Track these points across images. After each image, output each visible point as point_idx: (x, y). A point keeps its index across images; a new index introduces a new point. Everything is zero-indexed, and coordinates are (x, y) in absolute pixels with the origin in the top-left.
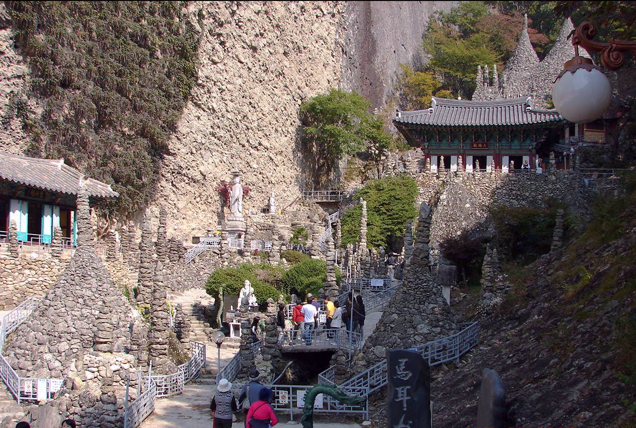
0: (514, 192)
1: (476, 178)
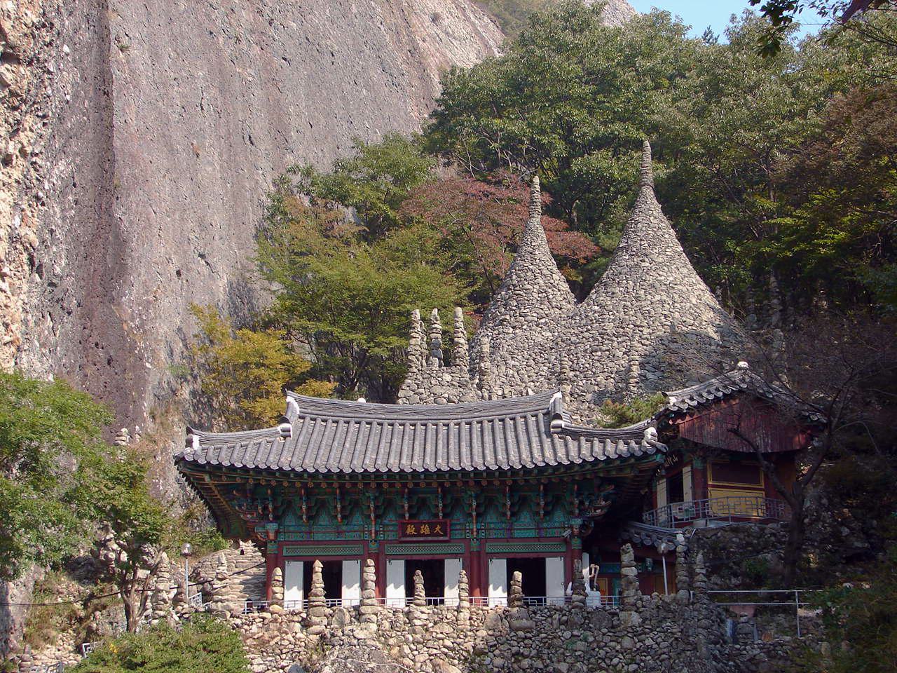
1: (417, 622)
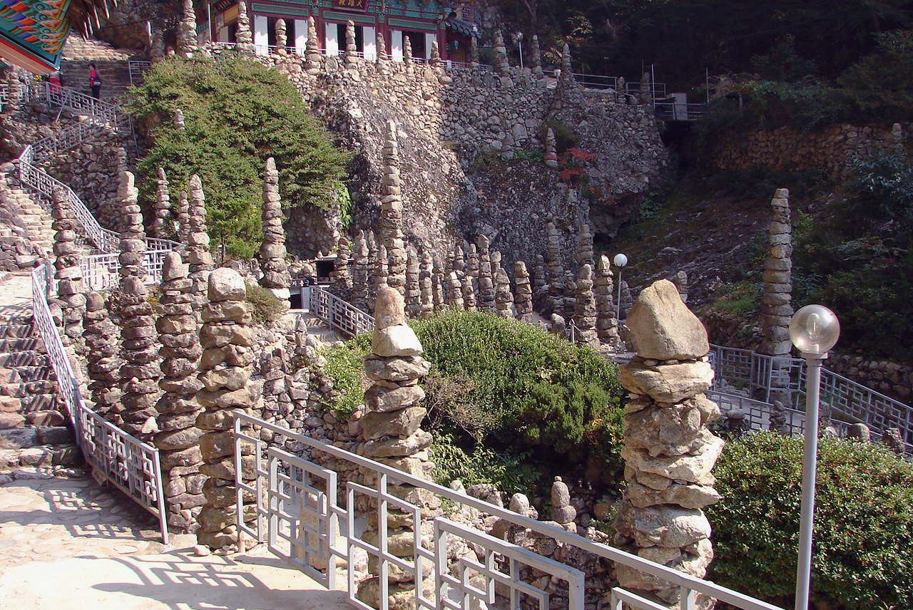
0: (452, 107)
1: (385, 72)
